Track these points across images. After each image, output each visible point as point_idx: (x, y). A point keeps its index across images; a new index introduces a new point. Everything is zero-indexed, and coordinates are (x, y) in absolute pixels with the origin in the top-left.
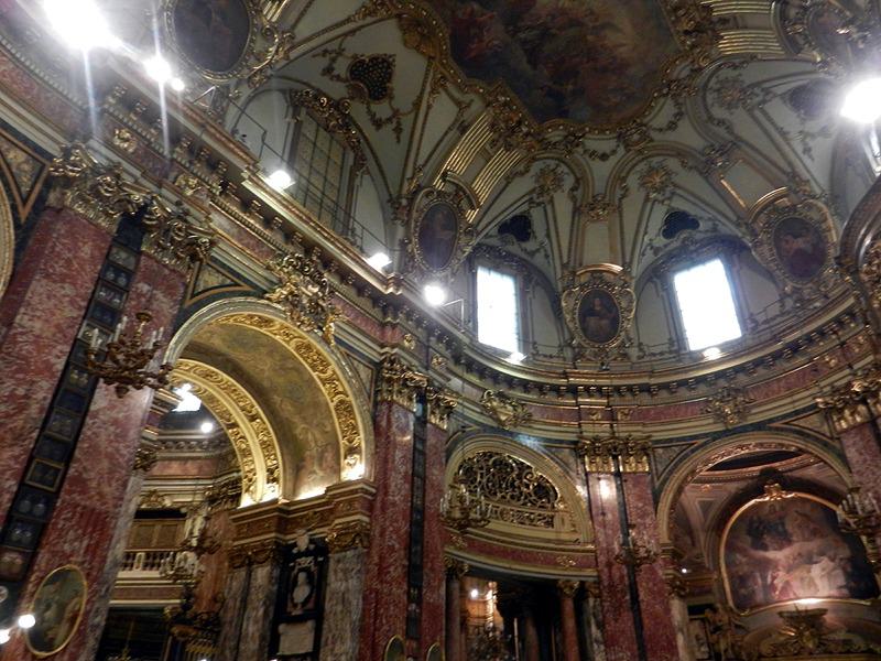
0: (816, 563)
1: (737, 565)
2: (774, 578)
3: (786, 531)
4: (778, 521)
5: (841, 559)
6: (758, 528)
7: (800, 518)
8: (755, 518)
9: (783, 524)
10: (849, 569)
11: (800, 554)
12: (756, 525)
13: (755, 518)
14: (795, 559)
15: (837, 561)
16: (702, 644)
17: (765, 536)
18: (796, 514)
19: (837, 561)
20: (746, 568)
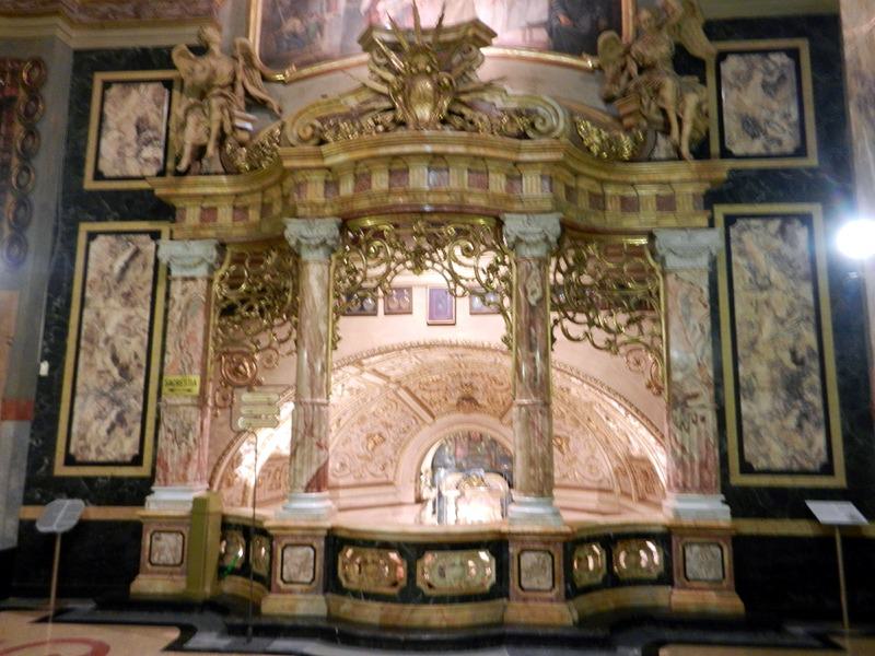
16: (148, 142)
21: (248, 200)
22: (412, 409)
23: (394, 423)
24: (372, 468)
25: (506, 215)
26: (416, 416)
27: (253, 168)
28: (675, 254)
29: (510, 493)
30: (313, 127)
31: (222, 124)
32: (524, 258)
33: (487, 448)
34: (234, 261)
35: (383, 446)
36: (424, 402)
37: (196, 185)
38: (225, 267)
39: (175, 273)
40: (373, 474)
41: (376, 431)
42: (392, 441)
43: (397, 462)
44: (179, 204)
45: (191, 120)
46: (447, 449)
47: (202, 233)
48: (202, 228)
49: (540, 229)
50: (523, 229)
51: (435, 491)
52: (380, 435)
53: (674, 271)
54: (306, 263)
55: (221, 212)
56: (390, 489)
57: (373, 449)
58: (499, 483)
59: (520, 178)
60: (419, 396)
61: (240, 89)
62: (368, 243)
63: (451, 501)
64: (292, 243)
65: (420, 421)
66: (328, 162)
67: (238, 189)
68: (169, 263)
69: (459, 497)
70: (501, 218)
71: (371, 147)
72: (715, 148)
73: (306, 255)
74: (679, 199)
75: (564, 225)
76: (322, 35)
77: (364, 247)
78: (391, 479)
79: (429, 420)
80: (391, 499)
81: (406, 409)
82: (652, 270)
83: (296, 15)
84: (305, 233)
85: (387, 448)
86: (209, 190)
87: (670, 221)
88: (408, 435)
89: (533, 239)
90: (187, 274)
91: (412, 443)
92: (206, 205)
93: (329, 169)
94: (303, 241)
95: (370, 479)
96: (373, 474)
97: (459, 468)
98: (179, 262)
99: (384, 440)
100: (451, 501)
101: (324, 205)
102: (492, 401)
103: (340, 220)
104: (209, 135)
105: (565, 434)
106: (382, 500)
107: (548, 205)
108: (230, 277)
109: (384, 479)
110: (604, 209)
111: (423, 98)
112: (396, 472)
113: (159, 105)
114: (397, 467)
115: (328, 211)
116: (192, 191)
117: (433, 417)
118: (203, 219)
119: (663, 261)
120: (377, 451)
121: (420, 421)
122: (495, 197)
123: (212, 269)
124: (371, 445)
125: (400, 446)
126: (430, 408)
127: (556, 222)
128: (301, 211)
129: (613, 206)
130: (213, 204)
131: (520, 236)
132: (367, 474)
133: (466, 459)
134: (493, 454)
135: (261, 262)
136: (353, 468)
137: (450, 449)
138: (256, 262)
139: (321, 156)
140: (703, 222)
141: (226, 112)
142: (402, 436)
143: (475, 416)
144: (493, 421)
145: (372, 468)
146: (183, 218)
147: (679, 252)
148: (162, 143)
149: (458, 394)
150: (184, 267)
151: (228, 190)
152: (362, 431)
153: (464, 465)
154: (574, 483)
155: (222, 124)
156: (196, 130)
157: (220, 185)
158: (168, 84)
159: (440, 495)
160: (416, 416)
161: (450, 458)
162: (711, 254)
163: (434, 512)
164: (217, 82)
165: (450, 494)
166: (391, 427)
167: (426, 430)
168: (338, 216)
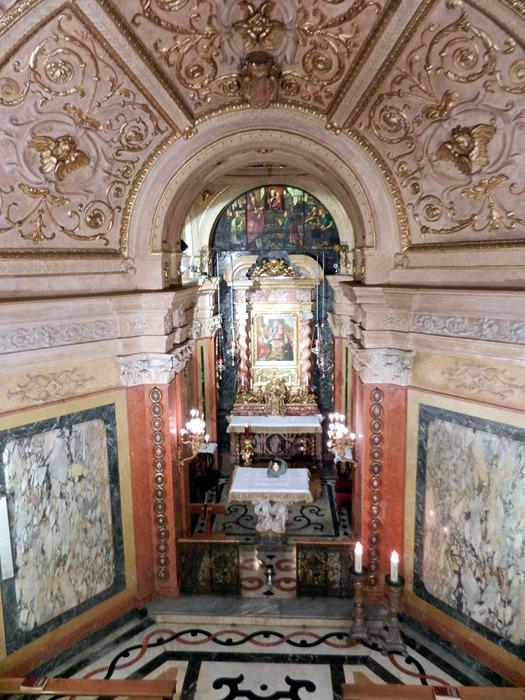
22: (141, 89)
23: (96, 115)
24: (65, 218)
26: (151, 105)
29: (325, 279)
33: (291, 219)
35: (85, 171)
36: (165, 68)
40: (70, 233)
41: (58, 132)
42: (106, 165)
43: (125, 213)
46: (233, 222)
51: (216, 281)
52: (72, 143)
56: (113, 264)
57: (59, 175)
58: (311, 268)
60: (147, 32)
63: (241, 295)
65: (163, 125)
69: (252, 290)
78: (114, 246)
79: (183, 122)
80: (114, 283)
81: (125, 83)
85: (93, 179)
88: (143, 156)
91: (152, 174)
95: (63, 242)
96: (70, 233)
97: (251, 249)
99: (83, 158)
100: (241, 295)
102: (312, 62)
105: (485, 119)
106: (96, 284)
109: (98, 244)
112: (122, 231)
114: (124, 221)
117: (191, 117)
120: (70, 177)
121: (163, 125)
124: (51, 165)
125: (126, 180)
126: (182, 90)
132: (57, 230)
133: (261, 235)
134: (300, 227)
136: (16, 218)
137: (237, 223)
142: (127, 155)
143: (278, 112)
144: (314, 121)
145: (65, 218)
149: (239, 47)
152: (14, 121)
153: (259, 245)
154: (486, 235)
159: (223, 284)
160: (151, 105)
161: (239, 237)
163: (216, 313)
165: (240, 285)
166: (95, 125)
167: (178, 144)
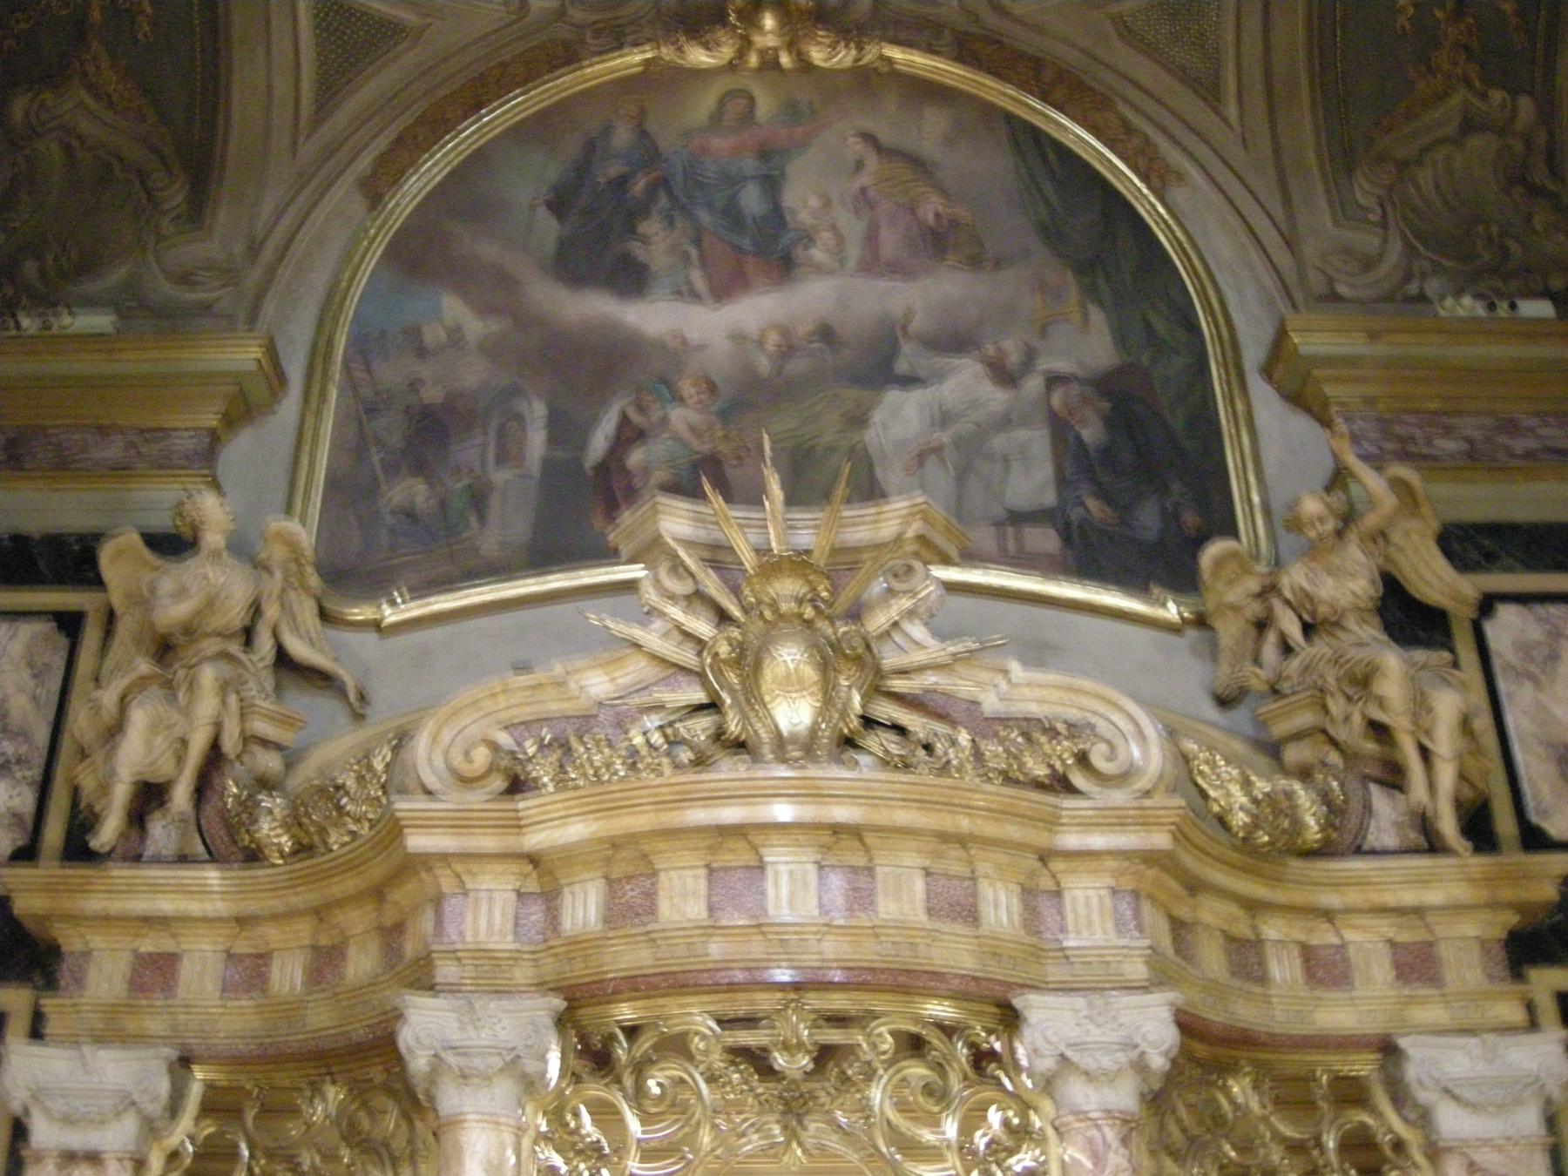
0: (910, 381)
1: (422, 352)
2: (629, 434)
3: (777, 217)
4: (750, 165)
5: (1053, 380)
6: (622, 182)
7: (872, 162)
8: (623, 136)
9: (772, 184)
10: (1091, 432)
11: (826, 334)
12: (615, 169)
13: (623, 136)
14: (788, 350)
15: (1033, 385)
17: (651, 227)
18: (855, 146)
19: (1033, 385)
20: (472, 374)
21: (272, 935)
25: (1033, 997)
27: (302, 849)
28: (1456, 1098)
30: (494, 747)
31: (218, 727)
32: (1080, 1114)
34: (209, 1108)
37: (131, 890)
38: (186, 1122)
39: (44, 1133)
44: (71, 940)
45: (139, 718)
47: (131, 1024)
48: (131, 1009)
49: (1112, 1036)
50: (1073, 1033)
53: (1460, 1147)
54: (456, 1122)
55: (188, 972)
59: (1058, 894)
61: (265, 645)
62: (640, 1069)
64: (419, 1063)
66: (535, 840)
67: (252, 906)
68: (26, 1111)
70: (1017, 1002)
71: (661, 804)
72: (1505, 824)
73: (451, 1099)
74: (1446, 952)
75: (1187, 1024)
76: (482, 519)
77: (628, 1081)
82: (1399, 1146)
83: (420, 468)
84: (455, 1036)
86: (167, 905)
87: (1433, 1013)
89: (1106, 1062)
90: (77, 1139)
92: (147, 946)
93: (533, 859)
94: (451, 1059)
98: (58, 1105)
101: (515, 958)
103: (558, 1003)
104: (180, 760)
107: (1137, 970)
108: (197, 1156)
110: (1263, 979)
111: (791, 683)
113: (38, 675)
115: (522, 974)
116: (118, 905)
118: (137, 984)
119: (1424, 1119)
122: (993, 950)
123: (151, 1129)
127: (1166, 1015)
128: (446, 971)
129: (1283, 969)
130: (166, 944)
131: (1069, 1053)
135: (294, 1111)
138: (276, 1110)
139: (517, 825)
140: (1512, 1012)
141: (233, 699)
146: (79, 981)
147: (1469, 1094)
148: (35, 772)
150: (69, 1120)
151: (218, 906)
155: (218, 727)
156: (148, 743)
157: (203, 892)
158: (70, 624)
162: (1548, 1102)
164: (217, 622)
168: (543, 987)
